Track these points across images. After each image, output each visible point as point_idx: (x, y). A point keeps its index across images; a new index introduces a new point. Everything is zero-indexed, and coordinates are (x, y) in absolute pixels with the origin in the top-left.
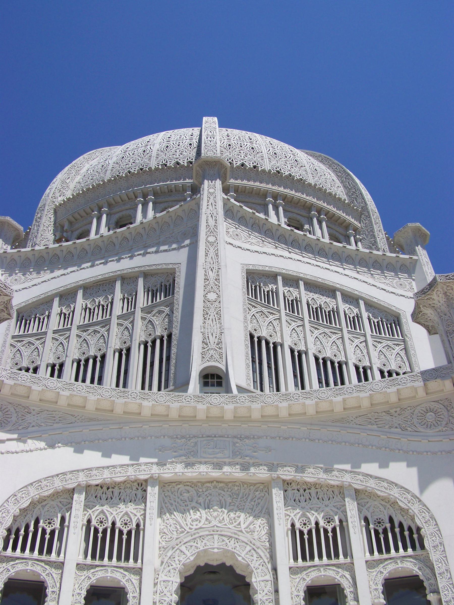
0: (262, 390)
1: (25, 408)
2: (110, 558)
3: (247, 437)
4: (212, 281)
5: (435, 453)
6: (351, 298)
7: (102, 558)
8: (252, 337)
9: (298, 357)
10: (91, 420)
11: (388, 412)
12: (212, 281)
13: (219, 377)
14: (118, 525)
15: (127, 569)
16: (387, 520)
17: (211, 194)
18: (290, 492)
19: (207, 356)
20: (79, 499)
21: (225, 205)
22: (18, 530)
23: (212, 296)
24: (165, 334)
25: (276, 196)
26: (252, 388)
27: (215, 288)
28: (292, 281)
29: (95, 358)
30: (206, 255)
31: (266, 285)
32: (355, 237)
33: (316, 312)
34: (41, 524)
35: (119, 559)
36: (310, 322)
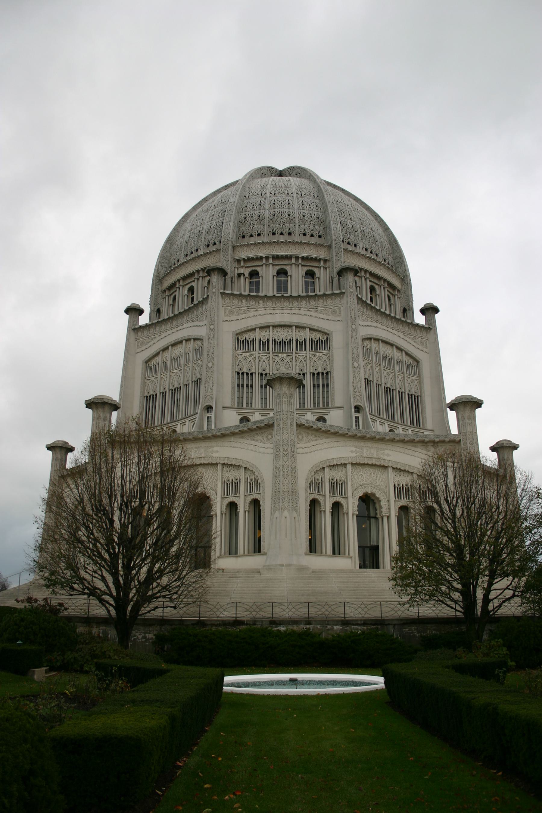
8: (238, 373)
12: (211, 354)
19: (207, 399)
23: (210, 365)
27: (212, 359)
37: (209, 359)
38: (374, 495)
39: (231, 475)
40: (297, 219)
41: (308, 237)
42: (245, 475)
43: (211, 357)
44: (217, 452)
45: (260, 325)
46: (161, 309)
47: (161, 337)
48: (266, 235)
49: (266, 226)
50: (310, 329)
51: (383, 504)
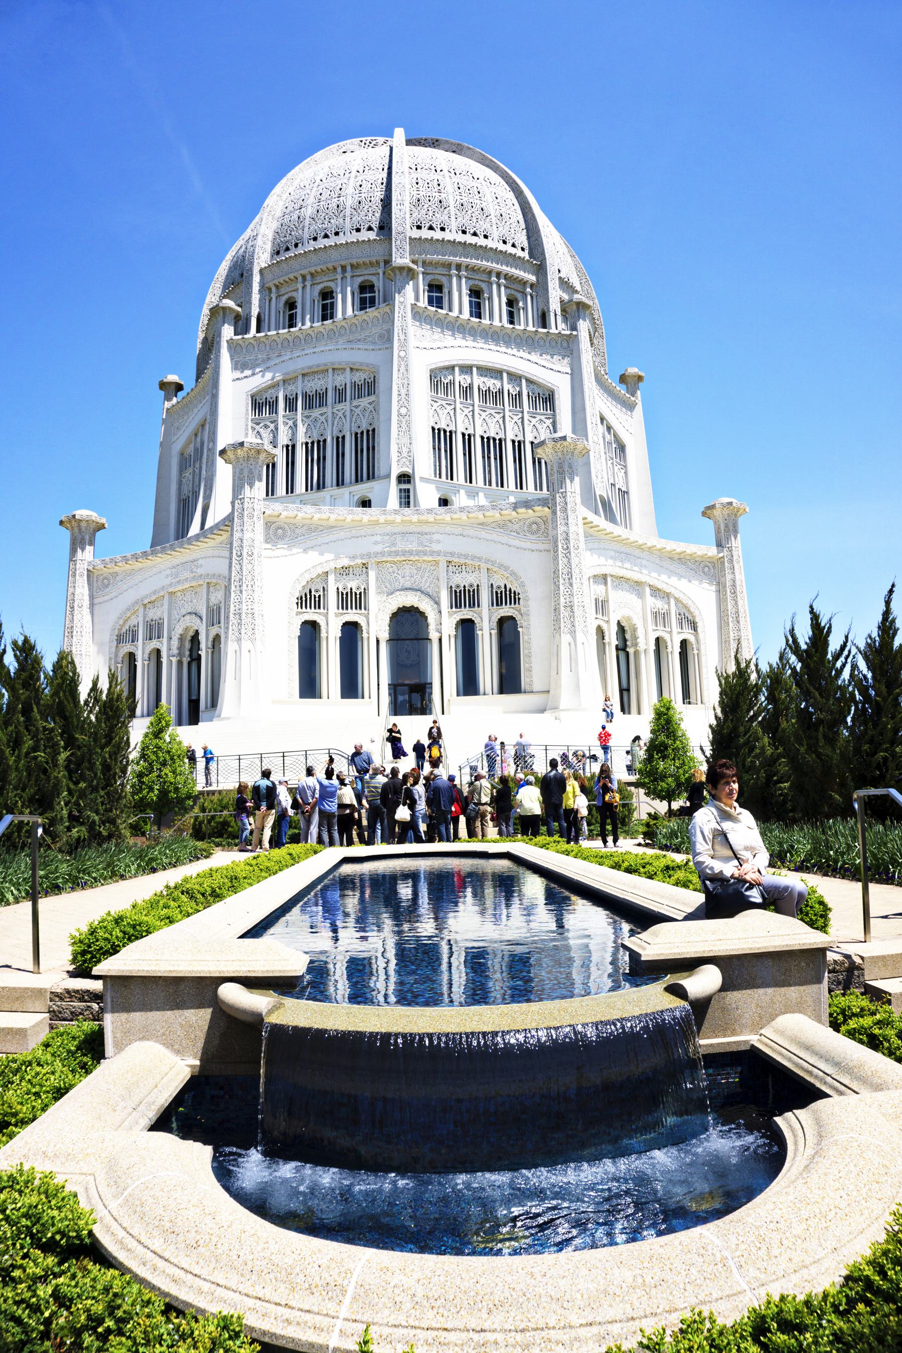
0: (440, 477)
1: (294, 525)
2: (352, 608)
3: (426, 534)
4: (403, 396)
5: (533, 551)
6: (515, 378)
7: (347, 608)
8: (433, 429)
9: (468, 439)
10: (333, 527)
11: (510, 521)
12: (403, 396)
13: (409, 476)
14: (354, 590)
15: (360, 614)
16: (503, 587)
17: (402, 303)
18: (450, 567)
19: (402, 462)
20: (331, 578)
21: (412, 309)
22: (301, 598)
23: (403, 411)
24: (370, 429)
25: (459, 267)
26: (433, 477)
27: (406, 402)
28: (466, 369)
29: (319, 442)
30: (399, 370)
31: (445, 377)
32: (531, 295)
33: (486, 394)
34: (313, 593)
35: (356, 608)
36: (479, 406)
37: (401, 402)
38: (629, 619)
39: (464, 580)
40: (492, 216)
41: (509, 245)
42: (489, 580)
43: (403, 400)
44: (438, 542)
45: (461, 362)
46: (262, 315)
47: (281, 359)
48: (454, 231)
49: (453, 218)
50: (528, 380)
51: (640, 633)
